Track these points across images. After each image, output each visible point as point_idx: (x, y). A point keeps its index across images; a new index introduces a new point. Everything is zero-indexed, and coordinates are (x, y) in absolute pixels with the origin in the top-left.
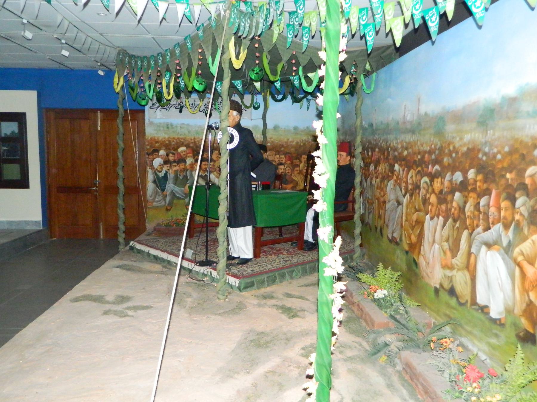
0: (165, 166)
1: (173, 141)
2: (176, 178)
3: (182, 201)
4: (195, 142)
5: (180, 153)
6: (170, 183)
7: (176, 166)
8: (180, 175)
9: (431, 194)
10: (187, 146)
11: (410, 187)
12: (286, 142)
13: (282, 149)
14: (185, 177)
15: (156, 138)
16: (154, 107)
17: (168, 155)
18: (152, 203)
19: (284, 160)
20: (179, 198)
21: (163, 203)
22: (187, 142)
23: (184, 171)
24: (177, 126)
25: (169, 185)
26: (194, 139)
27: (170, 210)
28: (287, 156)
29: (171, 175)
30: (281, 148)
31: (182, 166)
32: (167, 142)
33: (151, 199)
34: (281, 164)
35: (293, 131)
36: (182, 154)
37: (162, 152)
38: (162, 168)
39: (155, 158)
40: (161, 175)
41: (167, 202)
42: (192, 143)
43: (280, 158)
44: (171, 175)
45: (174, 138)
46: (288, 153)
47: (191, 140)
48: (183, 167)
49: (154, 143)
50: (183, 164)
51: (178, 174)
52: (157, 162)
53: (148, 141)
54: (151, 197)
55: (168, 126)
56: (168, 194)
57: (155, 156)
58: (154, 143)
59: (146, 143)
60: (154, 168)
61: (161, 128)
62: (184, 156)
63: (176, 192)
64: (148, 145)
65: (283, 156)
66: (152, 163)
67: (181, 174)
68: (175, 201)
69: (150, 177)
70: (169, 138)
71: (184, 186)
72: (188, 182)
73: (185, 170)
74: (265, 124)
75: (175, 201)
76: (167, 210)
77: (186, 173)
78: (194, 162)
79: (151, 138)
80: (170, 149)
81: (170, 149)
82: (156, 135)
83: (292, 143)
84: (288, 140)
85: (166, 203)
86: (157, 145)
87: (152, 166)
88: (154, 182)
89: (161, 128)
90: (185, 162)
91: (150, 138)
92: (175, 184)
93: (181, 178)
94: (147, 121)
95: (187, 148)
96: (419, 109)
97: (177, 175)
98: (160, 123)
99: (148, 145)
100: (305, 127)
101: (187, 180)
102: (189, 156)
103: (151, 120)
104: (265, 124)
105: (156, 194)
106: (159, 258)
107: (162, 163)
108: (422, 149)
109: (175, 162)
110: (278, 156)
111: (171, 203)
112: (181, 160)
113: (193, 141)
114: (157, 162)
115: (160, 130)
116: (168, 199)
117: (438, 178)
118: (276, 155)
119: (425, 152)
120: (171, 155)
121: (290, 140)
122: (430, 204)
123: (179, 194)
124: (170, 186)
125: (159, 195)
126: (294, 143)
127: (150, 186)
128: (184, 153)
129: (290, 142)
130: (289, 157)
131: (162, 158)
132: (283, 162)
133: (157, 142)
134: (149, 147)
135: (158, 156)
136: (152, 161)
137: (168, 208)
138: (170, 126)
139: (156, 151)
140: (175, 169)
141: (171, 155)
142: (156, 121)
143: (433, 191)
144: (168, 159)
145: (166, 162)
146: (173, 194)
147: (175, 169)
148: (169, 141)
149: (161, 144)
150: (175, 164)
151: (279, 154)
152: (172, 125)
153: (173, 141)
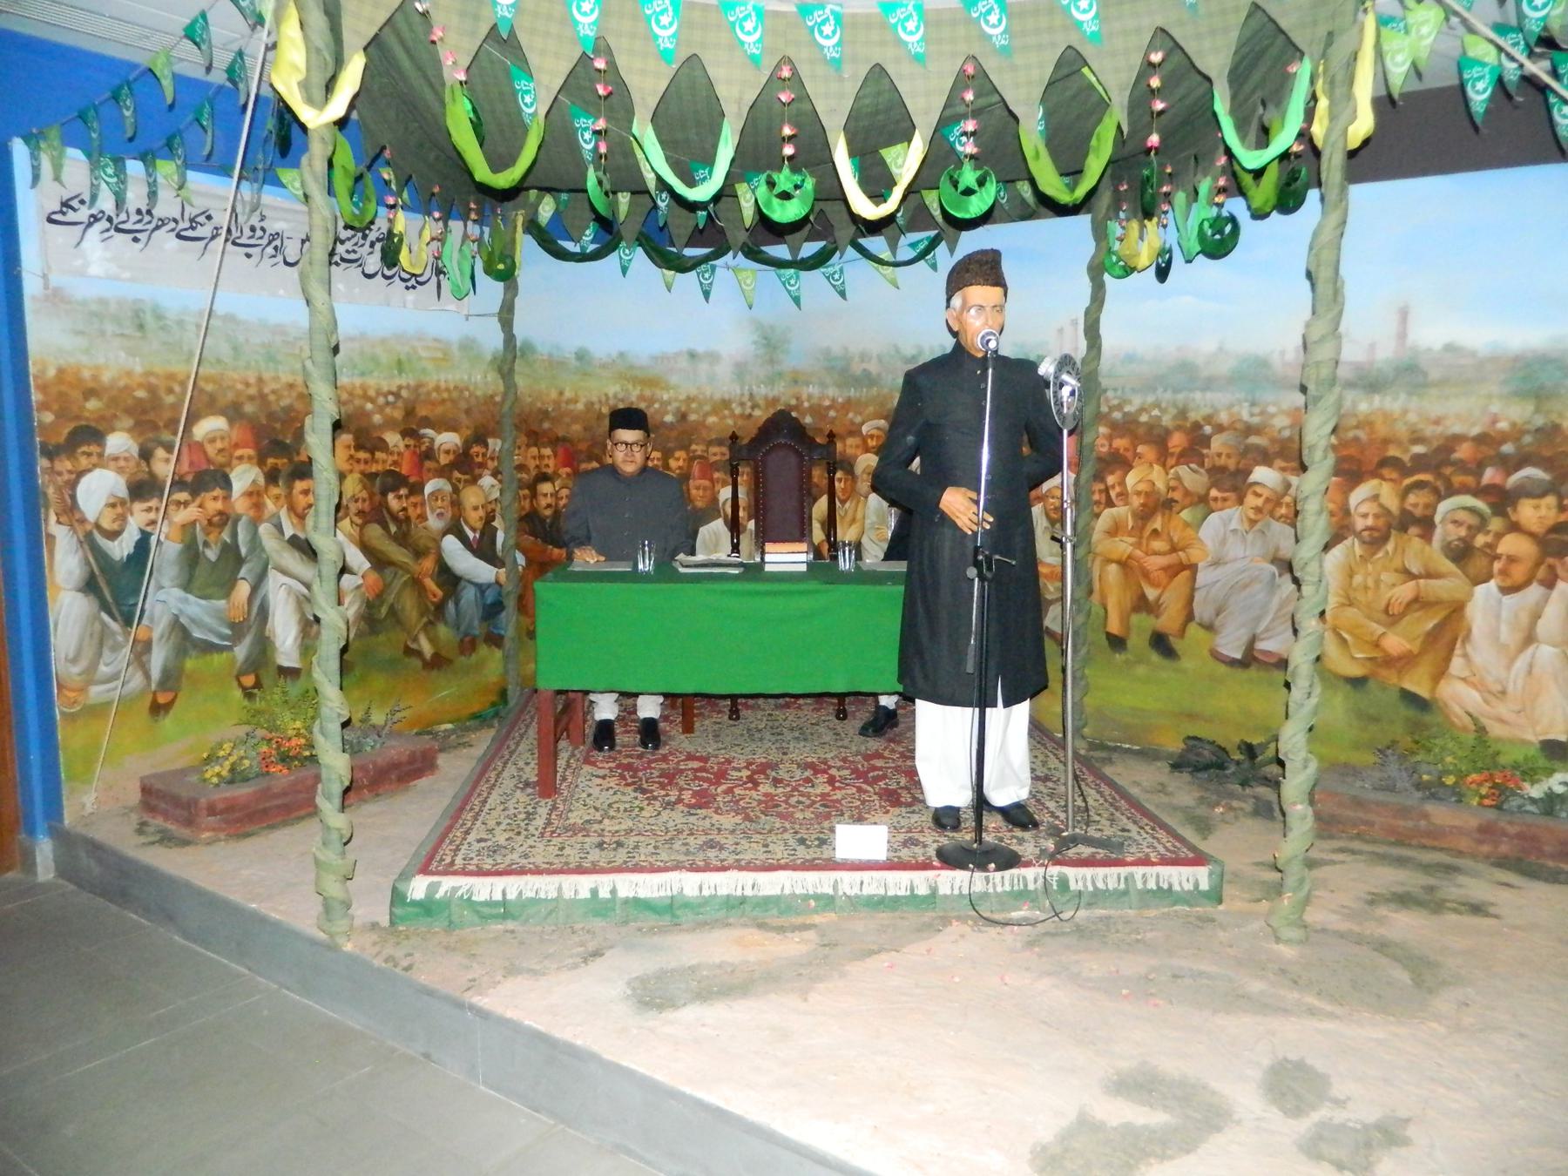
0: (138, 506)
1: (170, 391)
2: (191, 556)
3: (218, 659)
4: (262, 397)
5: (200, 445)
6: (166, 582)
7: (186, 504)
8: (206, 544)
9: (1499, 536)
10: (233, 412)
11: (1360, 524)
12: (557, 403)
13: (546, 425)
14: (231, 553)
15: (86, 374)
16: (71, 216)
17: (146, 455)
18: (83, 690)
19: (551, 462)
20: (208, 648)
21: (137, 681)
22: (230, 396)
23: (222, 525)
24: (180, 323)
25: (161, 595)
26: (260, 380)
27: (167, 707)
28: (560, 451)
29: (166, 552)
30: (541, 421)
31: (212, 503)
32: (141, 394)
33: (75, 670)
34: (544, 478)
35: (574, 363)
36: (211, 450)
37: (119, 442)
38: (122, 519)
39: (81, 474)
40: (120, 549)
41: (156, 674)
42: (251, 398)
43: (541, 457)
44: (166, 552)
45: (171, 377)
46: (564, 439)
47: (247, 385)
48: (219, 505)
49: (76, 395)
50: (218, 492)
51: (200, 537)
52: (98, 489)
53: (43, 388)
54: (74, 661)
55: (140, 321)
56: (156, 635)
57: (84, 462)
58: (76, 395)
59: (36, 397)
60: (83, 521)
61: (110, 328)
62: (221, 459)
63: (193, 621)
64: (44, 406)
65: (547, 451)
66: (73, 497)
67: (212, 538)
68: (190, 664)
69: (66, 562)
70: (149, 374)
71: (226, 587)
72: (242, 573)
73: (225, 519)
74: (510, 338)
75: (190, 664)
76: (157, 709)
77: (234, 535)
78: (261, 481)
79: (61, 371)
80: (155, 427)
81: (155, 427)
82: (84, 359)
83: (571, 407)
84: (561, 393)
85: (147, 676)
86: (93, 405)
87: (70, 510)
88: (89, 586)
89: (110, 328)
90: (227, 484)
91: (51, 372)
92: (187, 587)
93: (212, 554)
94: (31, 286)
95: (231, 421)
96: (1402, 335)
97: (194, 538)
98: (103, 302)
99: (44, 406)
100: (614, 354)
101: (240, 561)
102: (240, 458)
103: (55, 280)
104: (510, 338)
105: (102, 639)
106: (687, 905)
107: (123, 492)
108: (1429, 431)
109: (178, 484)
110: (534, 450)
111: (171, 678)
112: (207, 478)
113: (252, 391)
114: (98, 489)
115: (102, 333)
116: (158, 660)
117: (1543, 495)
118: (528, 446)
119: (1458, 439)
120: (160, 453)
121: (568, 394)
122: (1497, 557)
123: (211, 630)
124: (165, 599)
125: (116, 648)
126: (580, 406)
127: (69, 611)
128: (219, 445)
129: (568, 402)
130: (566, 450)
131: (120, 470)
132: (550, 471)
133: (90, 393)
134: (48, 417)
135: (101, 462)
136: (73, 485)
137: (162, 700)
138: (149, 319)
139: (90, 434)
140: (182, 516)
141: (160, 453)
142: (81, 290)
143: (1515, 527)
144: (151, 474)
145: (142, 488)
146: (179, 629)
147: (182, 516)
148: (152, 390)
149: (114, 401)
150: (183, 496)
151: (536, 445)
152: (159, 316)
153: (170, 391)
